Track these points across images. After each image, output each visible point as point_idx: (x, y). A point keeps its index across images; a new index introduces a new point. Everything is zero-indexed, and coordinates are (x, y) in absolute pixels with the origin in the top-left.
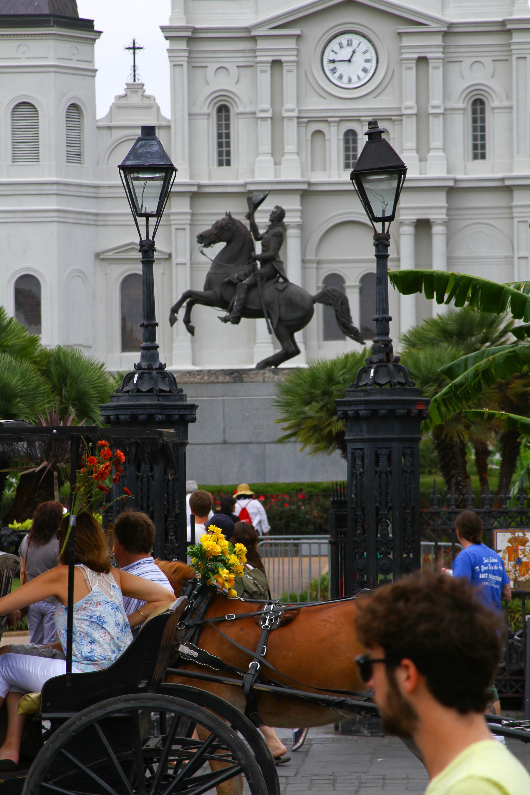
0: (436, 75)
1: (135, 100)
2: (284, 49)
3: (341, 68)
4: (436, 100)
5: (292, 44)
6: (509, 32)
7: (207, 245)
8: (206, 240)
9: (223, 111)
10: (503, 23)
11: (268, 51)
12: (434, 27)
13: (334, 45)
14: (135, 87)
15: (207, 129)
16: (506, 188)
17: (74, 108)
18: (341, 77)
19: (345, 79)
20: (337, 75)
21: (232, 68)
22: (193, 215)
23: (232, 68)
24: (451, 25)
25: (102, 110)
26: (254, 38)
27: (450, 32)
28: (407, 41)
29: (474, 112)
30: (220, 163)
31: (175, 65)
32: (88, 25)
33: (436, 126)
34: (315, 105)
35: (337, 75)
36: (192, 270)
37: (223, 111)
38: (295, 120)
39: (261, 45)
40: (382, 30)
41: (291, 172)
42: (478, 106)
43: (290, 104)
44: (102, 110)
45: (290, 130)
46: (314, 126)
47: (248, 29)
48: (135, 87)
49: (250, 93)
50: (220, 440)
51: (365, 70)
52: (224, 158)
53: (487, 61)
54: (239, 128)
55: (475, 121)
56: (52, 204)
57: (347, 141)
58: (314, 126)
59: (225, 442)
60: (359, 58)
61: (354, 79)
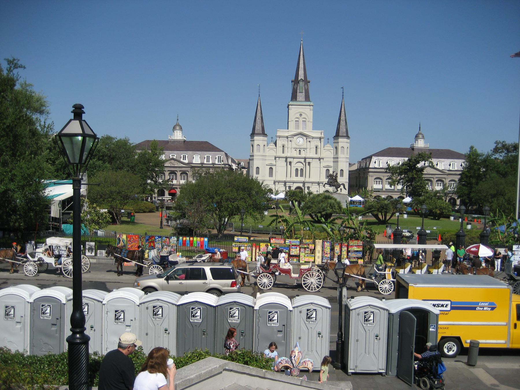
16: (320, 159)
27: (313, 138)
34: (295, 146)
46: (296, 149)
52: (283, 152)
54: (286, 149)
58: (296, 149)
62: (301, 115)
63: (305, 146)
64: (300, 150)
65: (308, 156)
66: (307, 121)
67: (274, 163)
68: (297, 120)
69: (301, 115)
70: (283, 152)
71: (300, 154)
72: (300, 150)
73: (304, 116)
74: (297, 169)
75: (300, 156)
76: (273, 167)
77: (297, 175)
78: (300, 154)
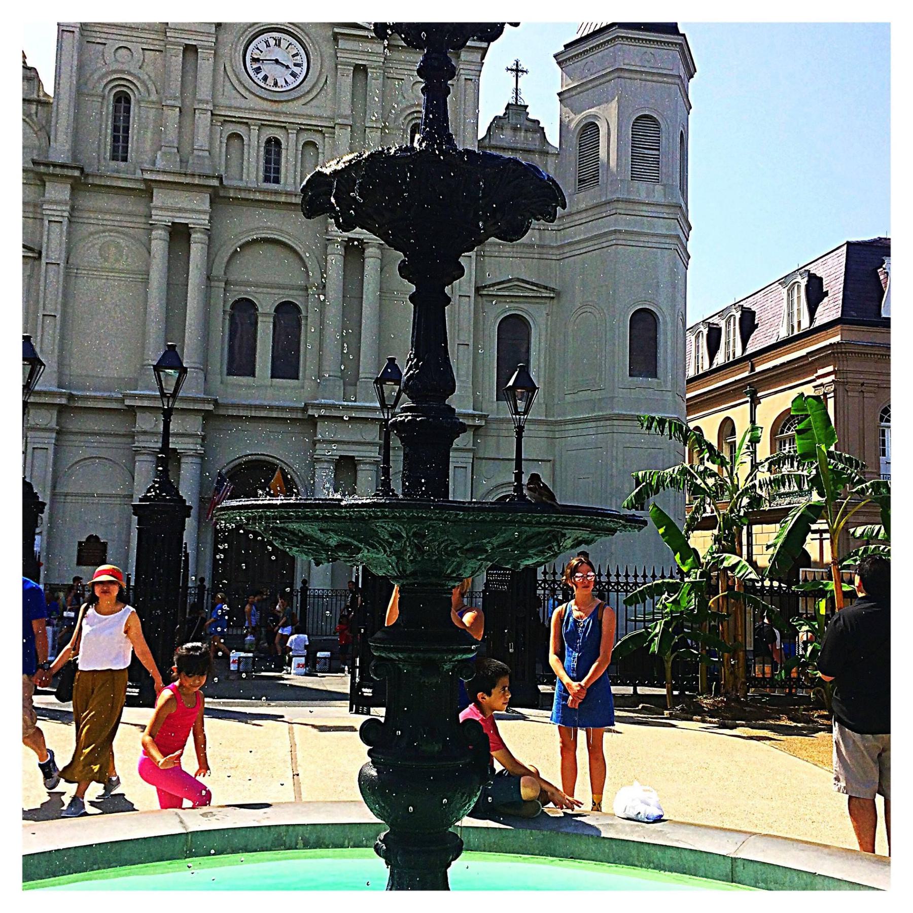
9: (122, 100)
15: (101, 115)
18: (265, 78)
19: (270, 81)
20: (261, 76)
21: (137, 48)
22: (73, 209)
23: (137, 48)
28: (342, 44)
30: (114, 158)
34: (233, 102)
35: (261, 76)
36: (67, 275)
38: (209, 113)
51: (294, 75)
57: (268, 152)
61: (281, 82)
64: (273, 145)
72: (273, 145)
77: (241, 362)
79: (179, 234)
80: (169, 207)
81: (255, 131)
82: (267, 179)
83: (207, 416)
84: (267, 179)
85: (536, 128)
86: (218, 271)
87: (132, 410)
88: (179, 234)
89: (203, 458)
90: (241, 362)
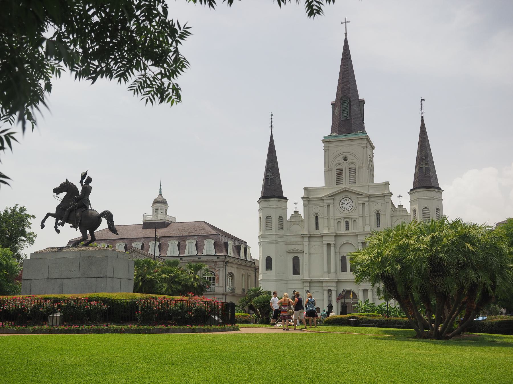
0: (367, 206)
1: (296, 215)
2: (330, 202)
3: (344, 205)
4: (367, 213)
5: (332, 201)
6: (384, 196)
7: (57, 194)
8: (57, 191)
9: (317, 217)
10: (383, 194)
11: (327, 202)
12: (366, 195)
13: (343, 201)
14: (296, 212)
15: (313, 221)
17: (281, 218)
21: (318, 207)
23: (318, 207)
24: (370, 195)
25: (288, 218)
26: (323, 200)
27: (370, 197)
28: (359, 199)
29: (377, 216)
31: (304, 207)
32: (285, 198)
33: (367, 219)
34: (338, 215)
36: (309, 255)
37: (317, 217)
39: (325, 201)
40: (354, 197)
41: (332, 231)
42: (378, 214)
43: (332, 214)
44: (288, 218)
45: (332, 221)
47: (321, 198)
48: (296, 212)
49: (322, 212)
50: (46, 277)
52: (317, 229)
53: (380, 203)
54: (320, 221)
55: (377, 218)
56: (274, 239)
59: (48, 278)
60: (349, 205)
62: (345, 159)
63: (355, 214)
64: (347, 222)
65: (360, 230)
66: (357, 169)
67: (299, 247)
68: (339, 167)
69: (345, 159)
70: (317, 229)
71: (347, 228)
72: (347, 222)
73: (351, 159)
74: (343, 259)
75: (347, 232)
76: (300, 256)
77: (344, 270)
78: (347, 228)
79: (329, 245)
80: (326, 240)
81: (343, 221)
82: (346, 229)
83: (337, 282)
84: (346, 229)
85: (405, 210)
86: (337, 251)
87: (322, 282)
88: (329, 245)
89: (337, 291)
90: (344, 270)
